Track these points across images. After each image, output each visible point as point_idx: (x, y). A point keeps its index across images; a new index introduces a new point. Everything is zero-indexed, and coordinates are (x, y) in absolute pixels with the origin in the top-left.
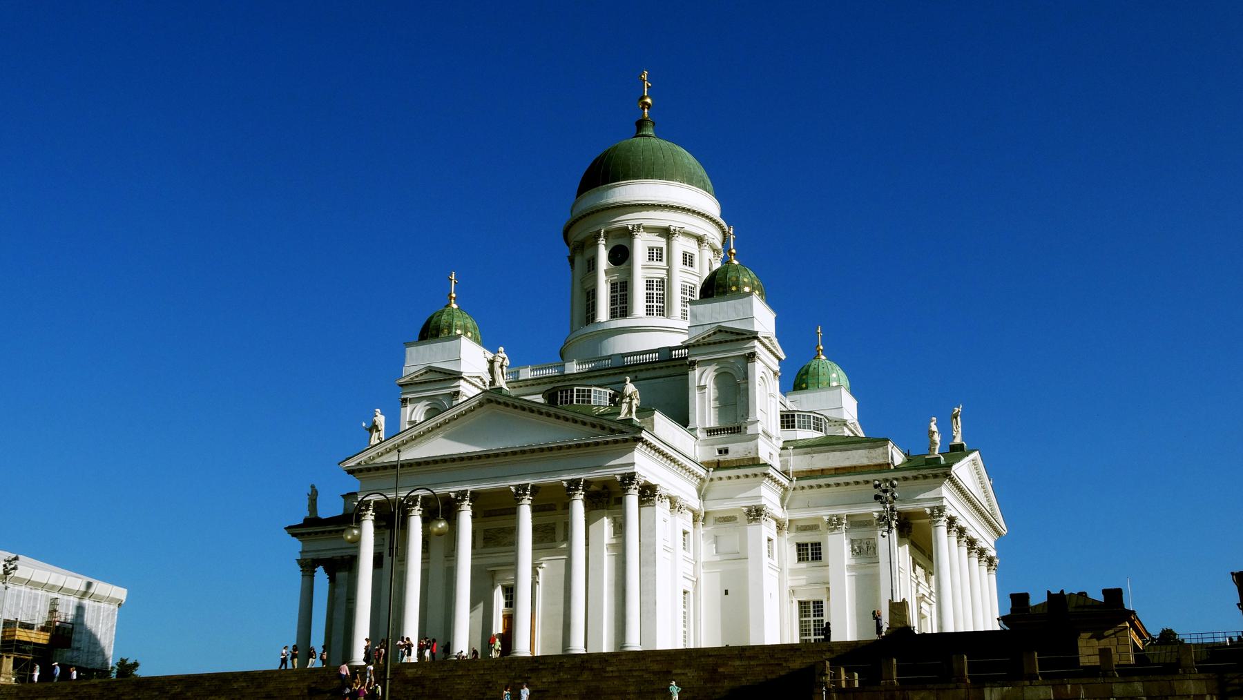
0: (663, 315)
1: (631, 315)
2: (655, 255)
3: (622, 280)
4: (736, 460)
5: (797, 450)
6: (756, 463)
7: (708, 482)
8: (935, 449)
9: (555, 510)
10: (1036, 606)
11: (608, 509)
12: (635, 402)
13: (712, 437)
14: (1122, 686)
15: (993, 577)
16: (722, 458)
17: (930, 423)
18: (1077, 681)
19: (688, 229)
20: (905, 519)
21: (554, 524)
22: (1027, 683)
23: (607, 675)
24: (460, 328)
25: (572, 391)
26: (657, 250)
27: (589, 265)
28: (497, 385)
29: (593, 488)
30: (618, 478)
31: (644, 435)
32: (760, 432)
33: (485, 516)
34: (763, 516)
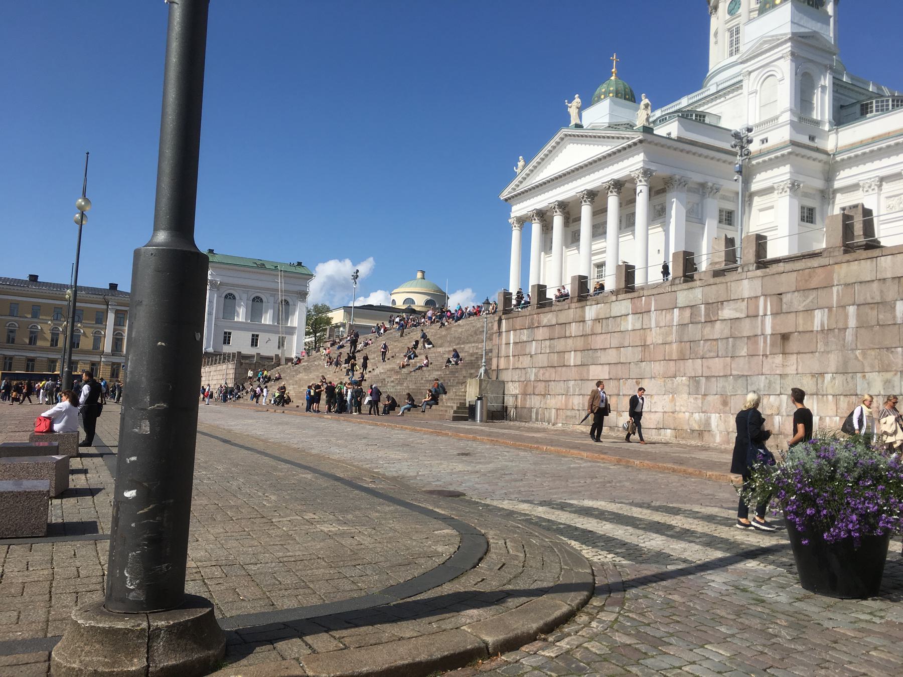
14: (685, 292)
16: (766, 145)
22: (614, 298)
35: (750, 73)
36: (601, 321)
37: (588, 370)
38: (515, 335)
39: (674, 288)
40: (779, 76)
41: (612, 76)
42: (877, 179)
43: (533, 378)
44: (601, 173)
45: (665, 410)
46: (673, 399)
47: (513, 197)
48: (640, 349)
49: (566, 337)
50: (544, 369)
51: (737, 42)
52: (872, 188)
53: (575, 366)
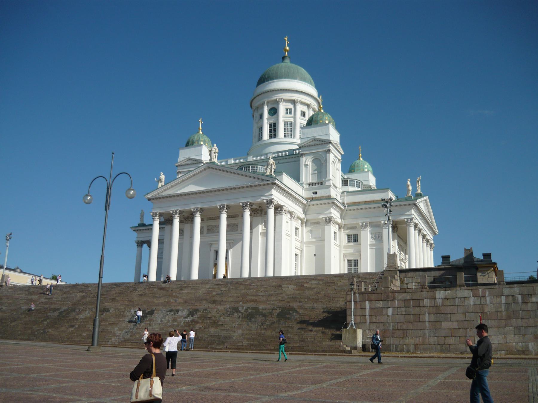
0: (292, 137)
1: (277, 137)
3: (274, 123)
4: (321, 197)
5: (348, 194)
6: (329, 198)
7: (308, 206)
8: (409, 193)
9: (238, 217)
10: (452, 261)
11: (261, 217)
12: (273, 167)
13: (310, 187)
14: (509, 289)
15: (432, 252)
16: (315, 196)
17: (407, 182)
18: (485, 287)
19: (303, 100)
20: (395, 224)
21: (238, 223)
22: (458, 288)
23: (252, 287)
24: (203, 141)
25: (249, 167)
26: (289, 110)
27: (260, 117)
28: (213, 160)
29: (254, 207)
30: (265, 201)
31: (277, 182)
32: (332, 184)
33: (208, 220)
34: (332, 222)
36: (449, 299)
38: (370, 304)
43: (391, 328)
45: (500, 342)
46: (505, 337)
49: (420, 306)
50: (401, 323)
53: (429, 322)
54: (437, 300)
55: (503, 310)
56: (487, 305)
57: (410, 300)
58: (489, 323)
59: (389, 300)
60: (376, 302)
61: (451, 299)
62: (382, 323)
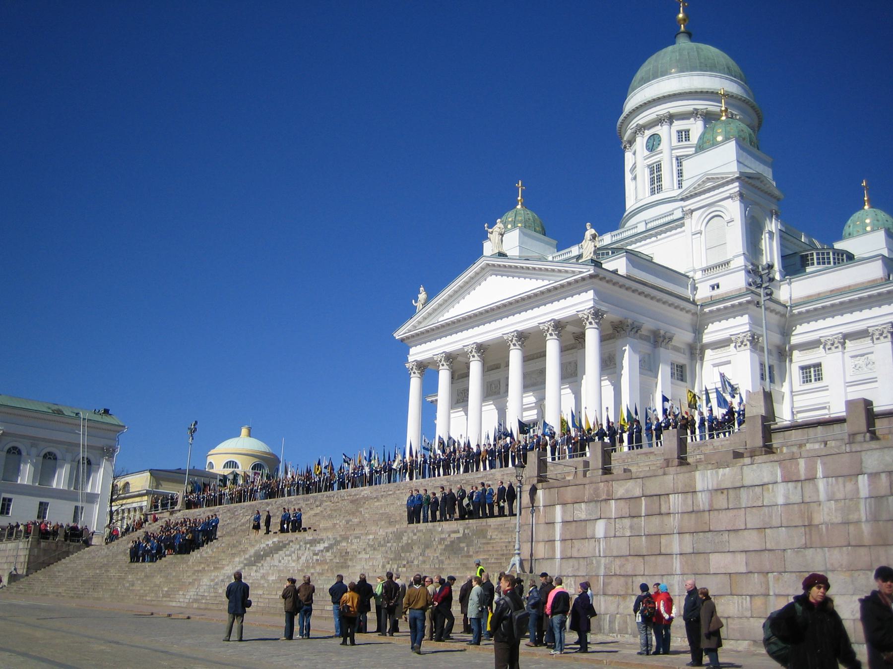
2: (684, 136)
16: (717, 292)
26: (685, 132)
29: (569, 328)
35: (692, 211)
36: (725, 492)
37: (708, 562)
38: (564, 512)
39: (856, 447)
40: (727, 218)
41: (518, 204)
42: (840, 336)
43: (602, 572)
44: (543, 309)
47: (413, 336)
48: (803, 529)
49: (660, 514)
50: (622, 559)
51: (659, 179)
52: (835, 345)
54: (699, 494)
55: (864, 519)
56: (820, 505)
57: (640, 497)
58: (825, 556)
59: (598, 501)
60: (575, 505)
61: (731, 491)
62: (584, 558)
